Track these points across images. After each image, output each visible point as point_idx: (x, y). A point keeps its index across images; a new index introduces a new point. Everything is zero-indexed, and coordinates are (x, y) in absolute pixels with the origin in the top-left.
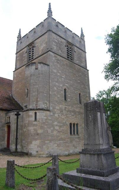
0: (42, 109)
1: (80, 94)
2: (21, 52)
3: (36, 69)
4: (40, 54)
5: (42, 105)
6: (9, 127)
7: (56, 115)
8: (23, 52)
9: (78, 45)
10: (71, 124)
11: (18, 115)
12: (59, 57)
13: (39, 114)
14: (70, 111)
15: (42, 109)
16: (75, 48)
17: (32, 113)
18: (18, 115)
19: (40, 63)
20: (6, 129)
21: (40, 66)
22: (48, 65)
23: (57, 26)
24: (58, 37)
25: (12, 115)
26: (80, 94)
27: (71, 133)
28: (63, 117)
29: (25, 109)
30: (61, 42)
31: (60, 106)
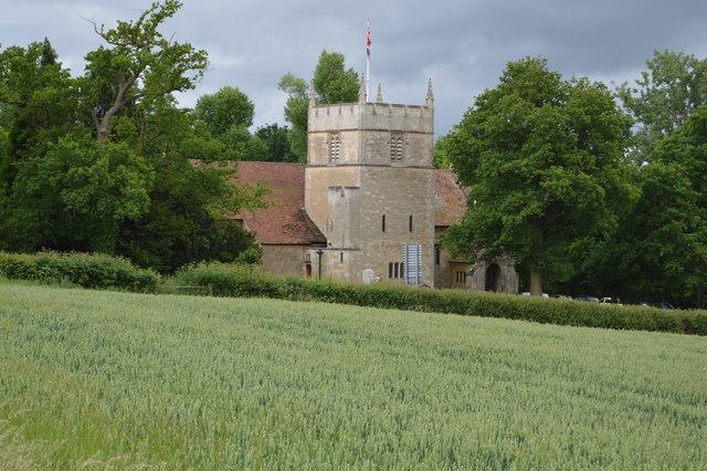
0: (350, 249)
1: (411, 217)
2: (318, 135)
3: (343, 196)
4: (347, 159)
5: (348, 244)
6: (309, 267)
7: (368, 254)
8: (322, 138)
9: (415, 128)
10: (391, 265)
11: (320, 253)
12: (375, 169)
13: (346, 255)
14: (392, 246)
15: (350, 249)
16: (409, 135)
17: (337, 253)
18: (320, 253)
19: (347, 188)
20: (305, 268)
21: (346, 192)
22: (357, 188)
23: (374, 113)
24: (375, 133)
25: (313, 253)
26: (411, 217)
27: (390, 276)
28: (378, 255)
29: (328, 246)
30: (382, 139)
31: (375, 241)
